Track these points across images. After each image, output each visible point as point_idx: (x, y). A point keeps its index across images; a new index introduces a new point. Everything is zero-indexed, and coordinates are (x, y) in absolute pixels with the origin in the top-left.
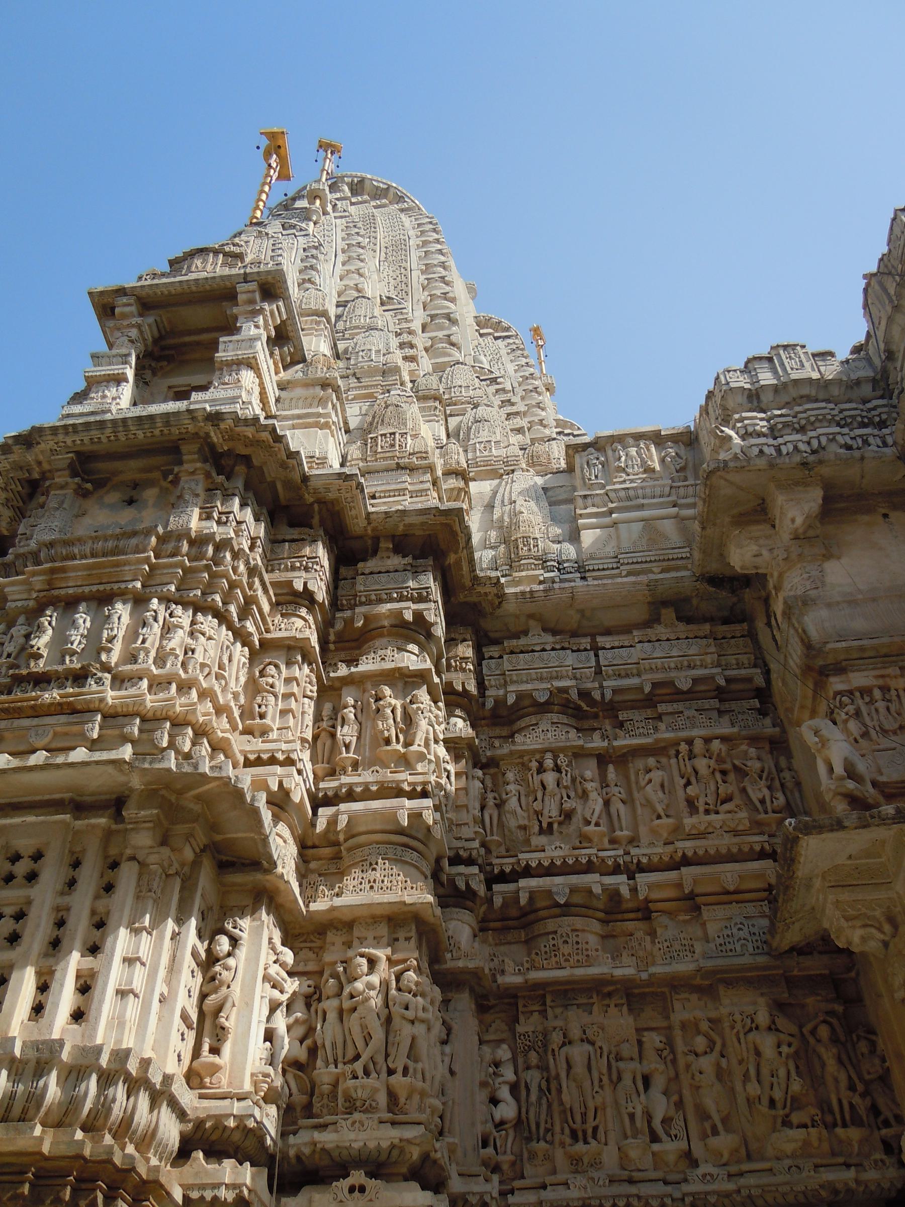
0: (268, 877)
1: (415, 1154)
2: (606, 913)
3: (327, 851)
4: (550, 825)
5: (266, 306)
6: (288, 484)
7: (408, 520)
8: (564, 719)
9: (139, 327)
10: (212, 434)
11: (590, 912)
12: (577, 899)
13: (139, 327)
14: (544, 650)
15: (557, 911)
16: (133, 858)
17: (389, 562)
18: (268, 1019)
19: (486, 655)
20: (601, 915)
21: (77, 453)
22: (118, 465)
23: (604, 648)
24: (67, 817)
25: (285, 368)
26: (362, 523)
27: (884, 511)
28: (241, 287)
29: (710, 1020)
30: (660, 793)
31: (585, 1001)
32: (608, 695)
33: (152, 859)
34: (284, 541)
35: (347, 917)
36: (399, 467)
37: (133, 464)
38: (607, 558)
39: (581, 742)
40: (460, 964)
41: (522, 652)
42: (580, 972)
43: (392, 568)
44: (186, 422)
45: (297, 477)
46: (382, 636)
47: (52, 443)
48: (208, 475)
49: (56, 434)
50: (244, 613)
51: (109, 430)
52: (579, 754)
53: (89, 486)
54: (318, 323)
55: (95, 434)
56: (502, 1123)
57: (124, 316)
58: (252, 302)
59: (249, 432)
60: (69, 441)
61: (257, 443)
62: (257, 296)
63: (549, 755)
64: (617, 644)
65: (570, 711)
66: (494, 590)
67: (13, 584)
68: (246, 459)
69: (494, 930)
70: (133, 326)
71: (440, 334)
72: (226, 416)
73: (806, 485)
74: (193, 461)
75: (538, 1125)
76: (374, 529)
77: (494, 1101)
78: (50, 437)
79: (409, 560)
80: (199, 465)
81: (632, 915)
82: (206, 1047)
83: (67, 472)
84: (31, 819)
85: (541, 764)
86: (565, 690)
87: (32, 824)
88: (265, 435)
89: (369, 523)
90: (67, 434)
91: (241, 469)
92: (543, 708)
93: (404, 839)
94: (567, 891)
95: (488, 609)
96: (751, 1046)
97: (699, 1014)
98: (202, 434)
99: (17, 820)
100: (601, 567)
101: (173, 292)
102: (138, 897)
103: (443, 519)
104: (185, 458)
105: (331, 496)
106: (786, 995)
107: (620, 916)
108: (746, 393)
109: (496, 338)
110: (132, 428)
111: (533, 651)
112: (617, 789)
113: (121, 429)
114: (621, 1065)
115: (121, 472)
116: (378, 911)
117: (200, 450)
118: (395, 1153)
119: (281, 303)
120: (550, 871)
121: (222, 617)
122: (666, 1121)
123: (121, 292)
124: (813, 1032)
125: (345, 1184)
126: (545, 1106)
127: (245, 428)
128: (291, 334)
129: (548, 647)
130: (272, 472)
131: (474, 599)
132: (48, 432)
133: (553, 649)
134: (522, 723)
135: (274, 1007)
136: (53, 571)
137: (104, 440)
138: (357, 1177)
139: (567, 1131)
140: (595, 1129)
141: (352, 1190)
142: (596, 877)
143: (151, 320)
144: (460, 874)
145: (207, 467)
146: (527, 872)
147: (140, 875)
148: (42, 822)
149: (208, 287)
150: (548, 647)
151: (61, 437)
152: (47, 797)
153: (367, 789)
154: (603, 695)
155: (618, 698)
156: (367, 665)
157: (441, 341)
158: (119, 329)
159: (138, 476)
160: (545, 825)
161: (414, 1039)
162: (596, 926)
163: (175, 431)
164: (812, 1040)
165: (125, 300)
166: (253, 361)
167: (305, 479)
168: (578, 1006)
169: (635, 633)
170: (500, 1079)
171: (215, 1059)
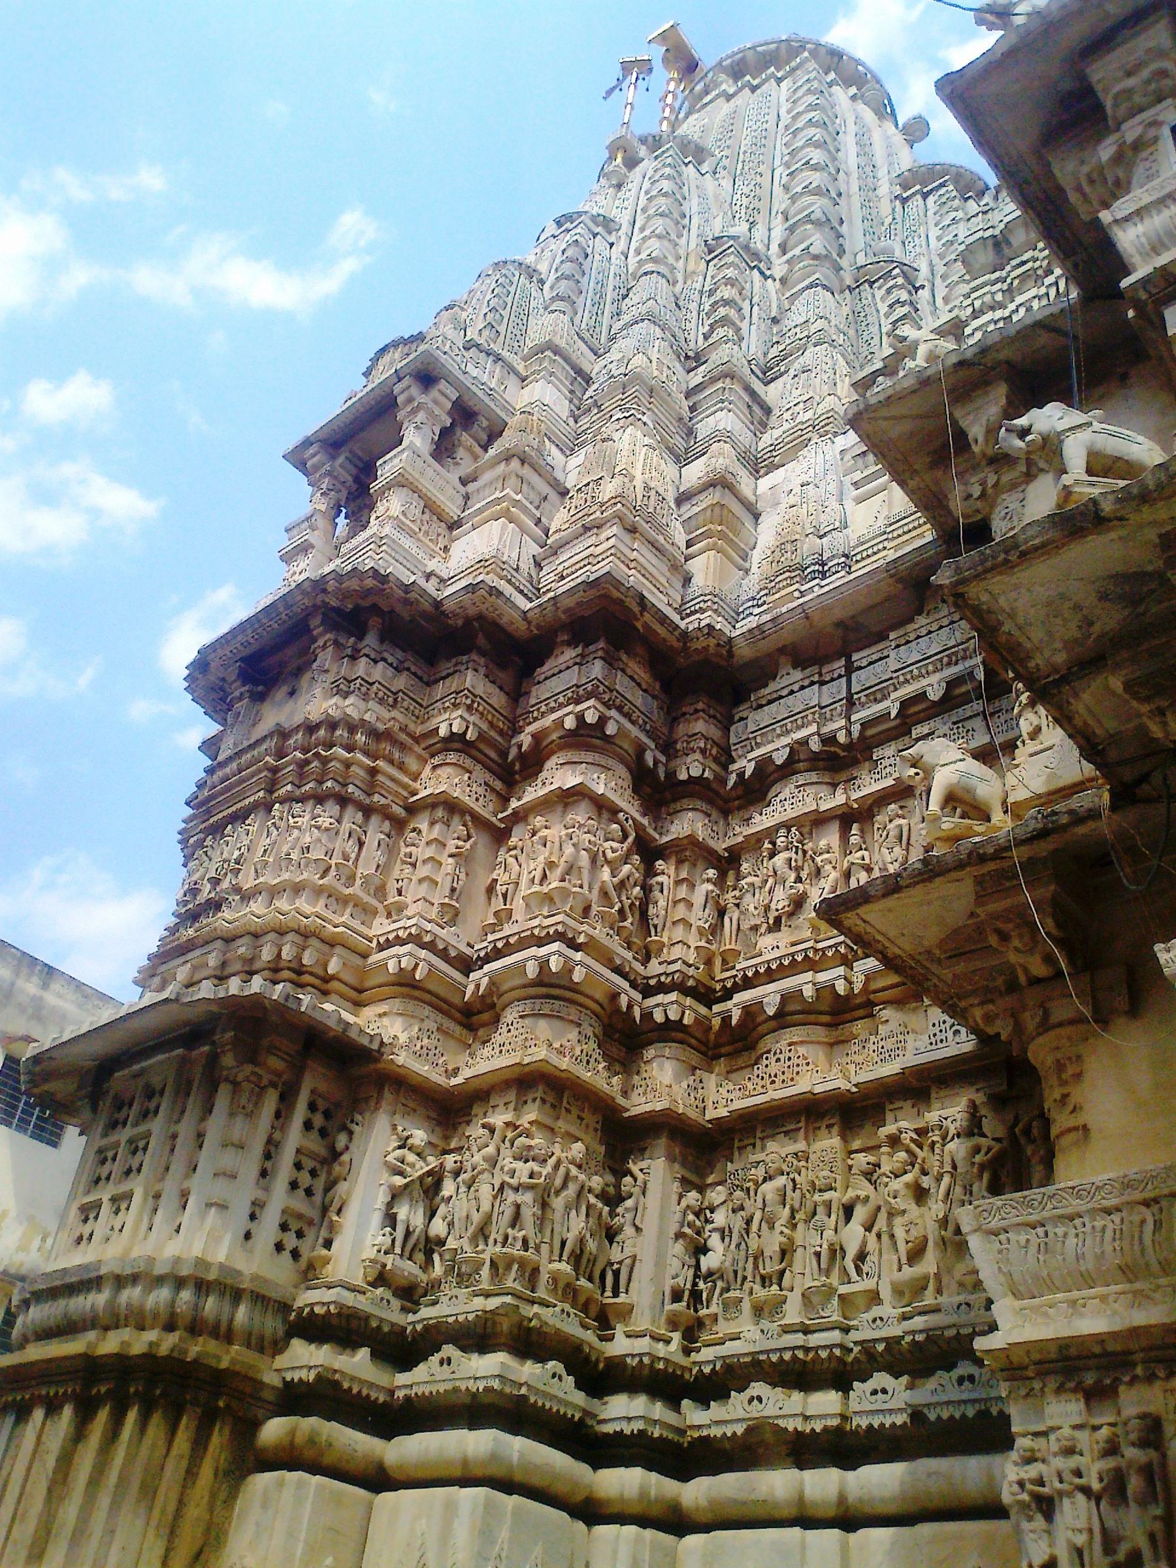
0: (381, 1066)
1: (505, 1325)
2: (831, 1013)
3: (485, 1017)
4: (778, 920)
5: (423, 399)
6: (424, 614)
8: (813, 777)
9: (329, 473)
11: (812, 1018)
12: (793, 1007)
13: (329, 473)
14: (792, 692)
15: (773, 1024)
16: (227, 1080)
17: (562, 659)
18: (390, 1205)
19: (737, 718)
20: (826, 1018)
21: (241, 659)
23: (860, 668)
24: (180, 1051)
25: (485, 448)
26: (523, 626)
27: (1120, 370)
28: (397, 389)
29: (916, 1131)
30: (897, 850)
31: (793, 1127)
32: (856, 729)
33: (240, 1078)
34: (437, 681)
35: (485, 1086)
36: (587, 529)
38: (874, 538)
39: (840, 799)
40: (648, 1108)
41: (770, 702)
42: (779, 1095)
43: (563, 667)
45: (426, 606)
46: (553, 753)
48: (336, 643)
50: (371, 788)
52: (818, 820)
53: (260, 688)
54: (541, 361)
55: (239, 638)
56: (710, 1274)
58: (410, 400)
59: (354, 584)
61: (369, 592)
62: (415, 391)
63: (782, 832)
64: (875, 657)
65: (821, 764)
66: (712, 642)
68: (375, 609)
69: (728, 1055)
71: (797, 251)
73: (987, 383)
75: (736, 1272)
76: (538, 627)
77: (703, 1249)
79: (579, 650)
81: (861, 1012)
82: (321, 1241)
83: (238, 683)
84: (161, 1057)
85: (774, 844)
86: (804, 742)
87: (161, 1062)
88: (370, 582)
89: (529, 623)
90: (222, 646)
91: (374, 622)
92: (788, 769)
93: (544, 990)
94: (778, 997)
95: (723, 663)
96: (947, 1159)
97: (903, 1124)
100: (870, 552)
102: (232, 1115)
103: (593, 593)
105: (472, 611)
106: (1004, 1087)
107: (848, 1016)
108: (990, 242)
109: (925, 196)
111: (781, 697)
112: (860, 854)
114: (817, 1197)
116: (508, 1075)
117: (323, 623)
118: (489, 1323)
119: (443, 385)
120: (771, 975)
121: (343, 801)
122: (861, 1256)
123: (307, 443)
124: (1027, 1131)
125: (435, 1359)
126: (743, 1253)
128: (476, 409)
129: (796, 687)
130: (404, 613)
131: (696, 658)
133: (802, 688)
134: (770, 795)
135: (396, 1195)
138: (448, 1350)
139: (758, 1279)
140: (782, 1273)
141: (442, 1363)
142: (809, 976)
143: (341, 459)
144: (658, 1005)
146: (748, 983)
147: (234, 1093)
150: (796, 687)
153: (507, 944)
154: (849, 732)
155: (870, 732)
156: (532, 793)
157: (800, 258)
159: (300, 661)
160: (771, 921)
161: (518, 1207)
162: (820, 1033)
164: (1023, 1141)
165: (311, 451)
167: (438, 604)
168: (786, 1133)
169: (892, 636)
170: (709, 1227)
171: (324, 1252)
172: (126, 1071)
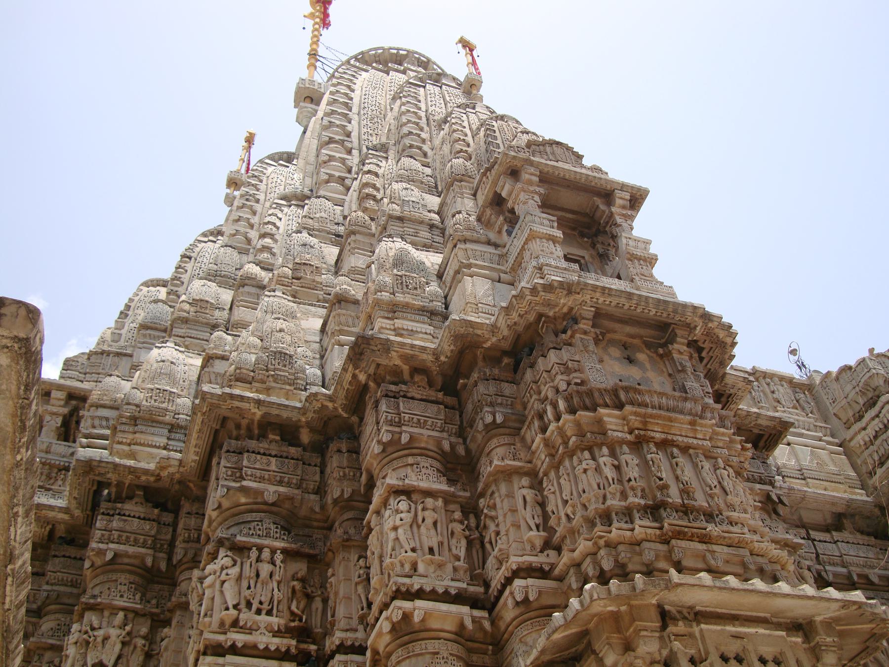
7: (760, 421)
10: (698, 328)
22: (617, 326)
28: (618, 193)
37: (628, 329)
44: (689, 314)
47: (588, 297)
49: (595, 291)
51: (635, 302)
55: (623, 300)
57: (530, 183)
59: (722, 334)
60: (601, 300)
67: (609, 415)
70: (536, 193)
72: (715, 319)
74: (683, 344)
78: (590, 292)
80: (685, 348)
83: (591, 323)
84: (761, 631)
98: (692, 326)
99: (752, 630)
101: (567, 177)
104: (678, 339)
110: (651, 305)
113: (643, 303)
115: (616, 332)
127: (721, 332)
132: (589, 288)
136: (644, 416)
137: (626, 307)
145: (691, 351)
148: (769, 635)
149: (593, 184)
151: (598, 295)
152: (754, 614)
158: (525, 191)
163: (678, 317)
165: (532, 170)
166: (653, 261)
172: (719, 628)
